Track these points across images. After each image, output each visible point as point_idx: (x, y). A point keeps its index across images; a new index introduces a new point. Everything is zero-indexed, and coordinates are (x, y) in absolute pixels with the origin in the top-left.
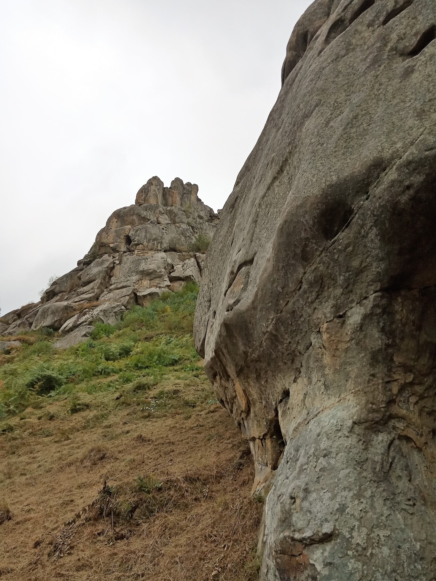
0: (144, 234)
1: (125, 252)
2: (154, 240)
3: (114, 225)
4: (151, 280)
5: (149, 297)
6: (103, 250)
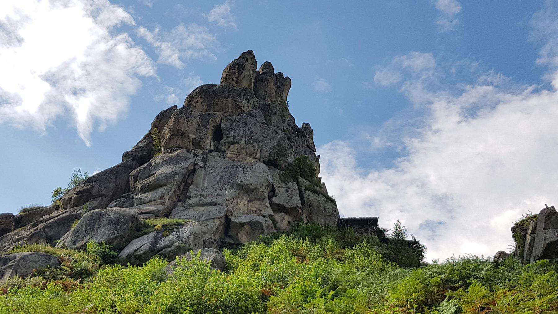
0: (242, 129)
1: (210, 151)
2: (255, 142)
3: (199, 108)
4: (250, 201)
5: (247, 227)
6: (177, 141)
